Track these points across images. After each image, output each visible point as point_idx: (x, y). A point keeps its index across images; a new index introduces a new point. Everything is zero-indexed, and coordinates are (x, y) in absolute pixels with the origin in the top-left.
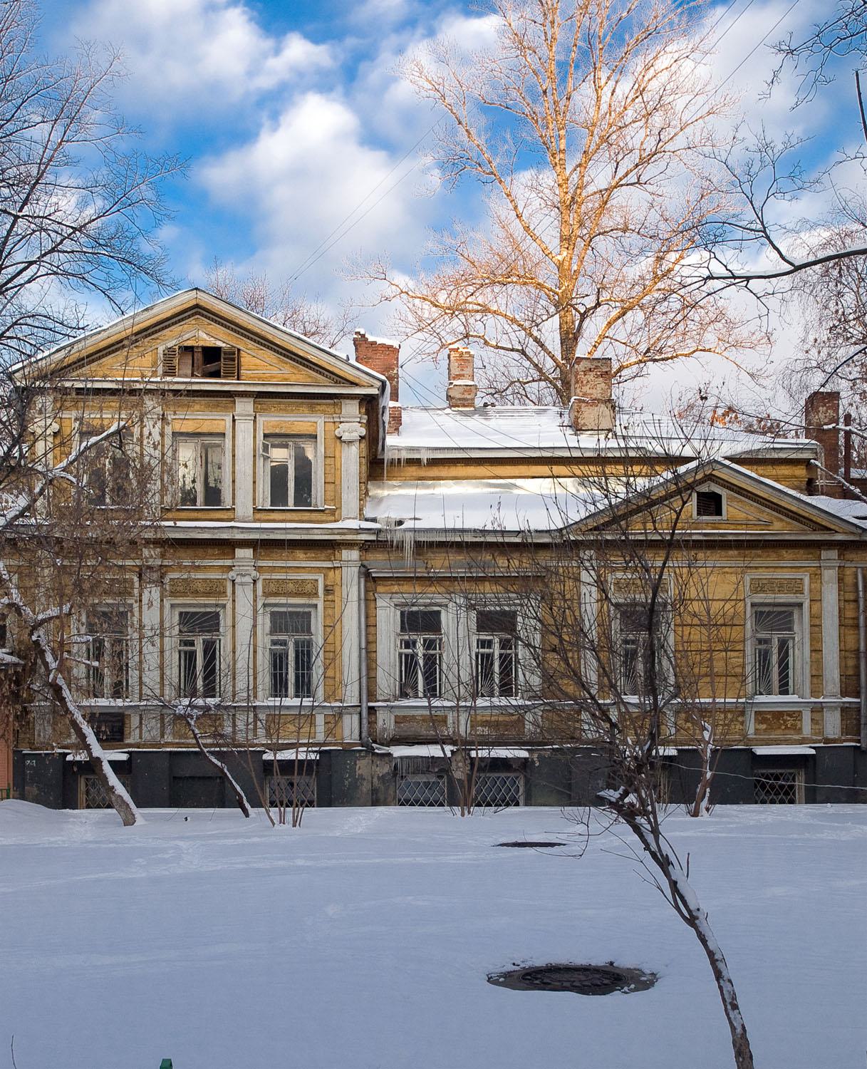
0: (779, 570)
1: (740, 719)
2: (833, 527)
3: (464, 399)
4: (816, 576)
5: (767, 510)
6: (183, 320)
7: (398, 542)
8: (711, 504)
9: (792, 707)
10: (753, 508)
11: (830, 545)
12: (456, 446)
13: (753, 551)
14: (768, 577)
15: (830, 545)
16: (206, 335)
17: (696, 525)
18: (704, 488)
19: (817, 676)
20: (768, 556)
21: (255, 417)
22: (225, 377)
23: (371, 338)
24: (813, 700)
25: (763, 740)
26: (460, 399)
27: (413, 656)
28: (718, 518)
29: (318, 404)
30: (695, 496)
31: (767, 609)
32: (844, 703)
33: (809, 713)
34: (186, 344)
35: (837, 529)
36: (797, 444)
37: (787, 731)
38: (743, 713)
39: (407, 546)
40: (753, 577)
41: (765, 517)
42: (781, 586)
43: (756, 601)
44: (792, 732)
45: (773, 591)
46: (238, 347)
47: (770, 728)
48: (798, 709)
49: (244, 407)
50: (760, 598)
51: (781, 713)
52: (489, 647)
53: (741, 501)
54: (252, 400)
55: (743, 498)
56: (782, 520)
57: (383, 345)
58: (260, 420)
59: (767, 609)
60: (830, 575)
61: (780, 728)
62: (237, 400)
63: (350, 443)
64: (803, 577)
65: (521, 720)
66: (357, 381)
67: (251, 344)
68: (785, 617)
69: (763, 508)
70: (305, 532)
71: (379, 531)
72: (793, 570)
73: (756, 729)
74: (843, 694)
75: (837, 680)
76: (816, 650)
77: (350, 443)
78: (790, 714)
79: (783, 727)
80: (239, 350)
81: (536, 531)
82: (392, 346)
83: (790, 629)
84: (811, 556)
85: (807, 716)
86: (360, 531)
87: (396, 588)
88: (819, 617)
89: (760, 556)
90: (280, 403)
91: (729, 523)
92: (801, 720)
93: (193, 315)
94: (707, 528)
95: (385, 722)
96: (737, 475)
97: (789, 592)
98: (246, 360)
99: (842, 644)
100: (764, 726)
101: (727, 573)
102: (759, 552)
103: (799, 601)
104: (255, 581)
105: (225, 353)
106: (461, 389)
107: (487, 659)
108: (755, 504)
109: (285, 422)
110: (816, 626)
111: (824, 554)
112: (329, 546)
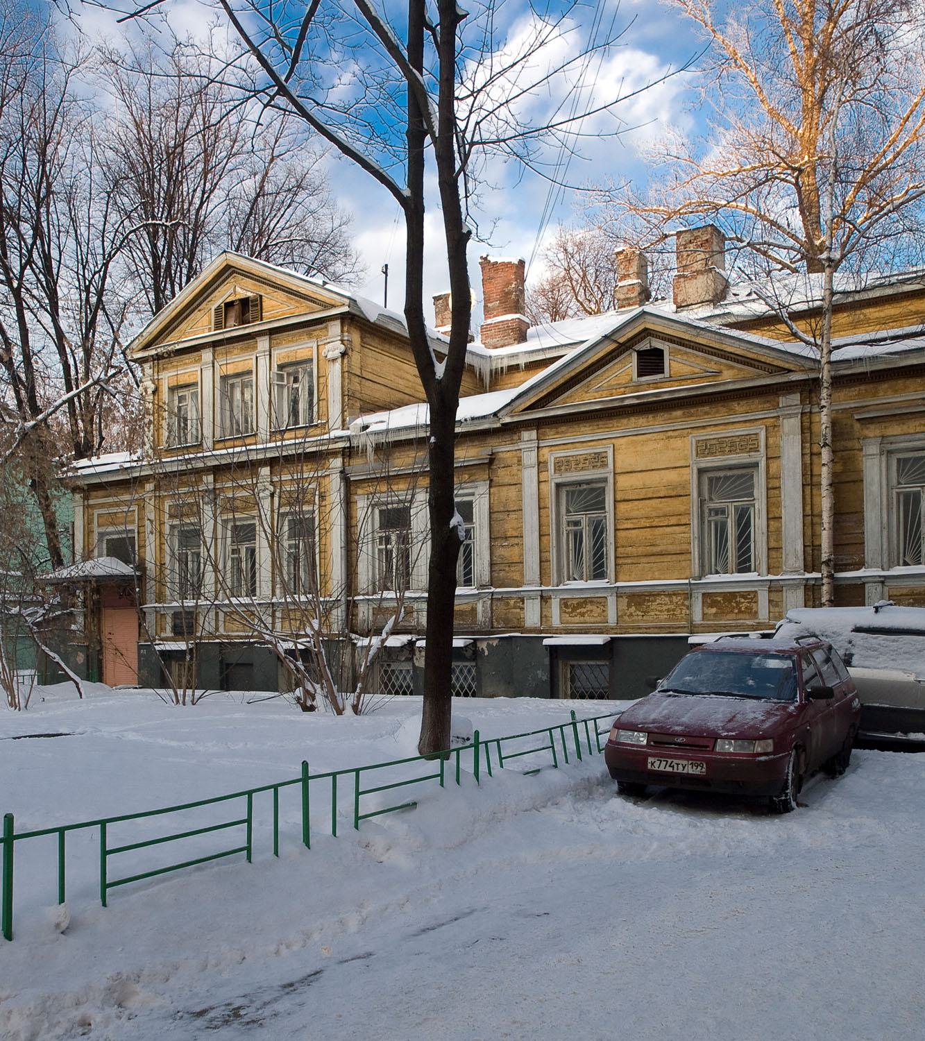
0: (731, 427)
1: (687, 603)
2: (787, 366)
3: (627, 299)
4: (773, 429)
5: (715, 358)
6: (224, 280)
7: (363, 446)
8: (651, 362)
9: (747, 586)
10: (698, 359)
11: (788, 388)
12: (558, 344)
14: (716, 436)
15: (788, 388)
16: (239, 289)
17: (638, 387)
18: (644, 346)
19: (774, 550)
20: (717, 412)
21: (270, 352)
22: (253, 322)
23: (492, 259)
24: (771, 577)
25: (709, 626)
26: (624, 299)
28: (661, 376)
29: (314, 330)
30: (635, 355)
31: (721, 474)
32: (807, 579)
33: (766, 594)
34: (228, 300)
35: (791, 367)
36: (916, 272)
37: (740, 616)
38: (688, 596)
39: (369, 449)
40: (698, 439)
41: (713, 367)
42: (732, 445)
43: (703, 465)
44: (747, 617)
45: (723, 452)
46: (260, 293)
47: (721, 613)
48: (753, 589)
49: (263, 343)
50: (708, 462)
51: (734, 595)
53: (686, 353)
54: (267, 337)
55: (688, 350)
56: (732, 367)
57: (503, 264)
58: (275, 353)
59: (721, 474)
60: (791, 425)
61: (732, 612)
62: (258, 339)
64: (757, 431)
65: (474, 610)
66: (333, 303)
67: (269, 289)
68: (746, 482)
69: (710, 357)
71: (349, 438)
72: (747, 424)
73: (704, 614)
74: (806, 569)
75: (800, 553)
76: (773, 518)
77: (334, 360)
78: (744, 595)
79: (736, 611)
80: (261, 296)
81: (473, 419)
82: (510, 263)
83: (752, 495)
84: (768, 405)
85: (763, 597)
86: (336, 440)
88: (778, 478)
89: (707, 413)
90: (288, 336)
91: (671, 380)
93: (231, 274)
94: (653, 387)
95: (364, 613)
96: (672, 324)
97: (742, 451)
98: (267, 303)
99: (808, 508)
100: (714, 610)
101: (671, 437)
102: (706, 408)
103: (753, 460)
104: (272, 495)
105: (252, 301)
106: (625, 290)
107: (389, 553)
108: (701, 354)
109: (291, 351)
110: (773, 489)
111: (783, 401)
112: (316, 458)
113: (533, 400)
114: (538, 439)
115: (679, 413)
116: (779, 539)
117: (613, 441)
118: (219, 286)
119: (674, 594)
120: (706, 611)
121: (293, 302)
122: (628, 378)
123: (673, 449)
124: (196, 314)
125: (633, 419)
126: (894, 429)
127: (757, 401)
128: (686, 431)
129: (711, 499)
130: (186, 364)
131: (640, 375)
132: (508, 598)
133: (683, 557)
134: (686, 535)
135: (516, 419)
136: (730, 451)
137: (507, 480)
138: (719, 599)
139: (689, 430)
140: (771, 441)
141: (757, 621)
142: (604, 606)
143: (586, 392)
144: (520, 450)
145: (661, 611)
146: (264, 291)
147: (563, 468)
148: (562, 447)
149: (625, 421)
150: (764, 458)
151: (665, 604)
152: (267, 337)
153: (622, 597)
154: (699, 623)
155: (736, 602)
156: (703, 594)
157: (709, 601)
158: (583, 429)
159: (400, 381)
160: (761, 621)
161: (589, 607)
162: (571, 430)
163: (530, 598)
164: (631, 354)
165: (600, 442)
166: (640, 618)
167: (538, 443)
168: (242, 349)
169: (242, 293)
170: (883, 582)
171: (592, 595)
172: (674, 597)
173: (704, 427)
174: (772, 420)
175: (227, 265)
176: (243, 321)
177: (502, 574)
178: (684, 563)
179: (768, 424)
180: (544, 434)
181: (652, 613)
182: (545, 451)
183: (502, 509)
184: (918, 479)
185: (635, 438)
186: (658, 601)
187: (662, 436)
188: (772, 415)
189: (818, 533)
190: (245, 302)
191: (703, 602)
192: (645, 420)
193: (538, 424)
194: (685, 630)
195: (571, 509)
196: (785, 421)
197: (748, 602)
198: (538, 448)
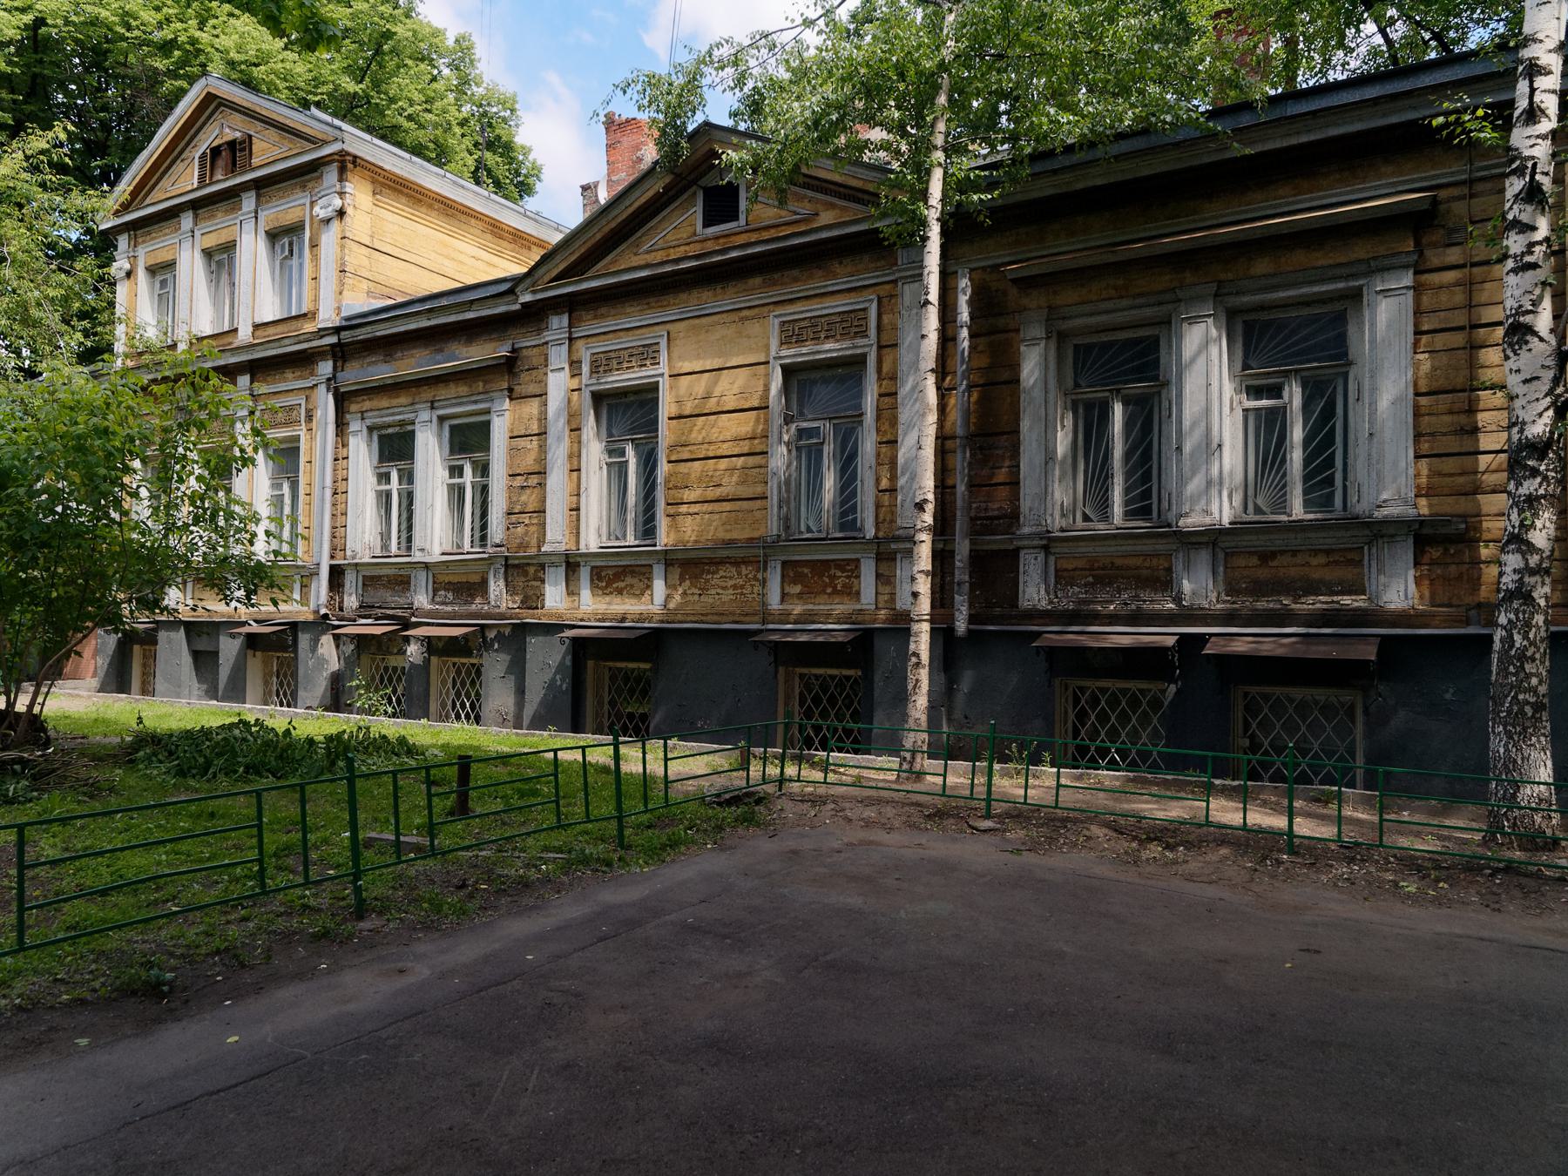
1: (760, 576)
5: (809, 193)
8: (722, 205)
13: (786, 273)
21: (256, 212)
27: (388, 494)
33: (872, 563)
34: (214, 144)
44: (846, 599)
50: (792, 354)
52: (461, 476)
54: (253, 193)
56: (832, 206)
58: (262, 215)
61: (824, 592)
63: (328, 221)
66: (324, 137)
70: (277, 344)
77: (328, 221)
79: (829, 590)
84: (883, 263)
87: (367, 405)
92: (858, 577)
98: (257, 146)
100: (797, 589)
102: (795, 273)
105: (240, 143)
113: (562, 267)
114: (570, 326)
115: (757, 281)
116: (893, 478)
117: (669, 327)
118: (204, 124)
119: (744, 563)
120: (787, 590)
121: (286, 142)
122: (690, 229)
123: (749, 337)
124: (179, 167)
125: (695, 293)
126: (1068, 297)
127: (866, 258)
128: (766, 309)
129: (801, 414)
130: (166, 235)
131: (705, 226)
132: (528, 564)
133: (758, 503)
134: (762, 470)
135: (540, 296)
136: (826, 337)
137: (533, 389)
138: (806, 571)
139: (771, 307)
140: (886, 319)
141: (859, 607)
142: (648, 579)
143: (635, 254)
144: (547, 343)
145: (724, 588)
146: (254, 128)
147: (601, 369)
148: (603, 337)
149: (683, 296)
150: (875, 348)
151: (731, 578)
152: (253, 193)
153: (672, 565)
154: (776, 607)
155: (829, 576)
156: (784, 563)
157: (791, 574)
158: (629, 310)
159: (446, 262)
160: (864, 607)
161: (629, 580)
162: (613, 312)
163: (553, 565)
164: (695, 193)
165: (651, 329)
166: (696, 597)
167: (570, 333)
168: (226, 211)
169: (230, 135)
170: (1046, 548)
171: (633, 563)
172: (743, 567)
173: (791, 301)
174: (887, 287)
175: (208, 93)
176: (233, 169)
177: (520, 530)
178: (758, 514)
179: (882, 294)
180: (580, 320)
181: (713, 592)
182: (580, 344)
183: (522, 433)
184: (1109, 377)
185: (697, 321)
186: (722, 573)
187: (734, 316)
188: (887, 279)
189: (950, 466)
190: (232, 144)
191: (783, 576)
192: (710, 293)
193: (574, 305)
194: (756, 618)
195: (614, 432)
196: (906, 287)
197: (847, 577)
198: (571, 339)
